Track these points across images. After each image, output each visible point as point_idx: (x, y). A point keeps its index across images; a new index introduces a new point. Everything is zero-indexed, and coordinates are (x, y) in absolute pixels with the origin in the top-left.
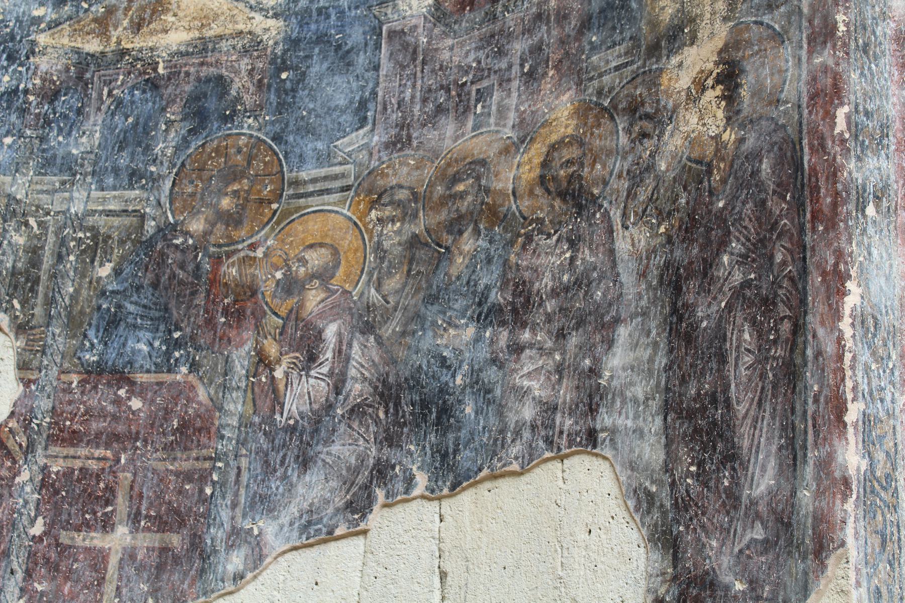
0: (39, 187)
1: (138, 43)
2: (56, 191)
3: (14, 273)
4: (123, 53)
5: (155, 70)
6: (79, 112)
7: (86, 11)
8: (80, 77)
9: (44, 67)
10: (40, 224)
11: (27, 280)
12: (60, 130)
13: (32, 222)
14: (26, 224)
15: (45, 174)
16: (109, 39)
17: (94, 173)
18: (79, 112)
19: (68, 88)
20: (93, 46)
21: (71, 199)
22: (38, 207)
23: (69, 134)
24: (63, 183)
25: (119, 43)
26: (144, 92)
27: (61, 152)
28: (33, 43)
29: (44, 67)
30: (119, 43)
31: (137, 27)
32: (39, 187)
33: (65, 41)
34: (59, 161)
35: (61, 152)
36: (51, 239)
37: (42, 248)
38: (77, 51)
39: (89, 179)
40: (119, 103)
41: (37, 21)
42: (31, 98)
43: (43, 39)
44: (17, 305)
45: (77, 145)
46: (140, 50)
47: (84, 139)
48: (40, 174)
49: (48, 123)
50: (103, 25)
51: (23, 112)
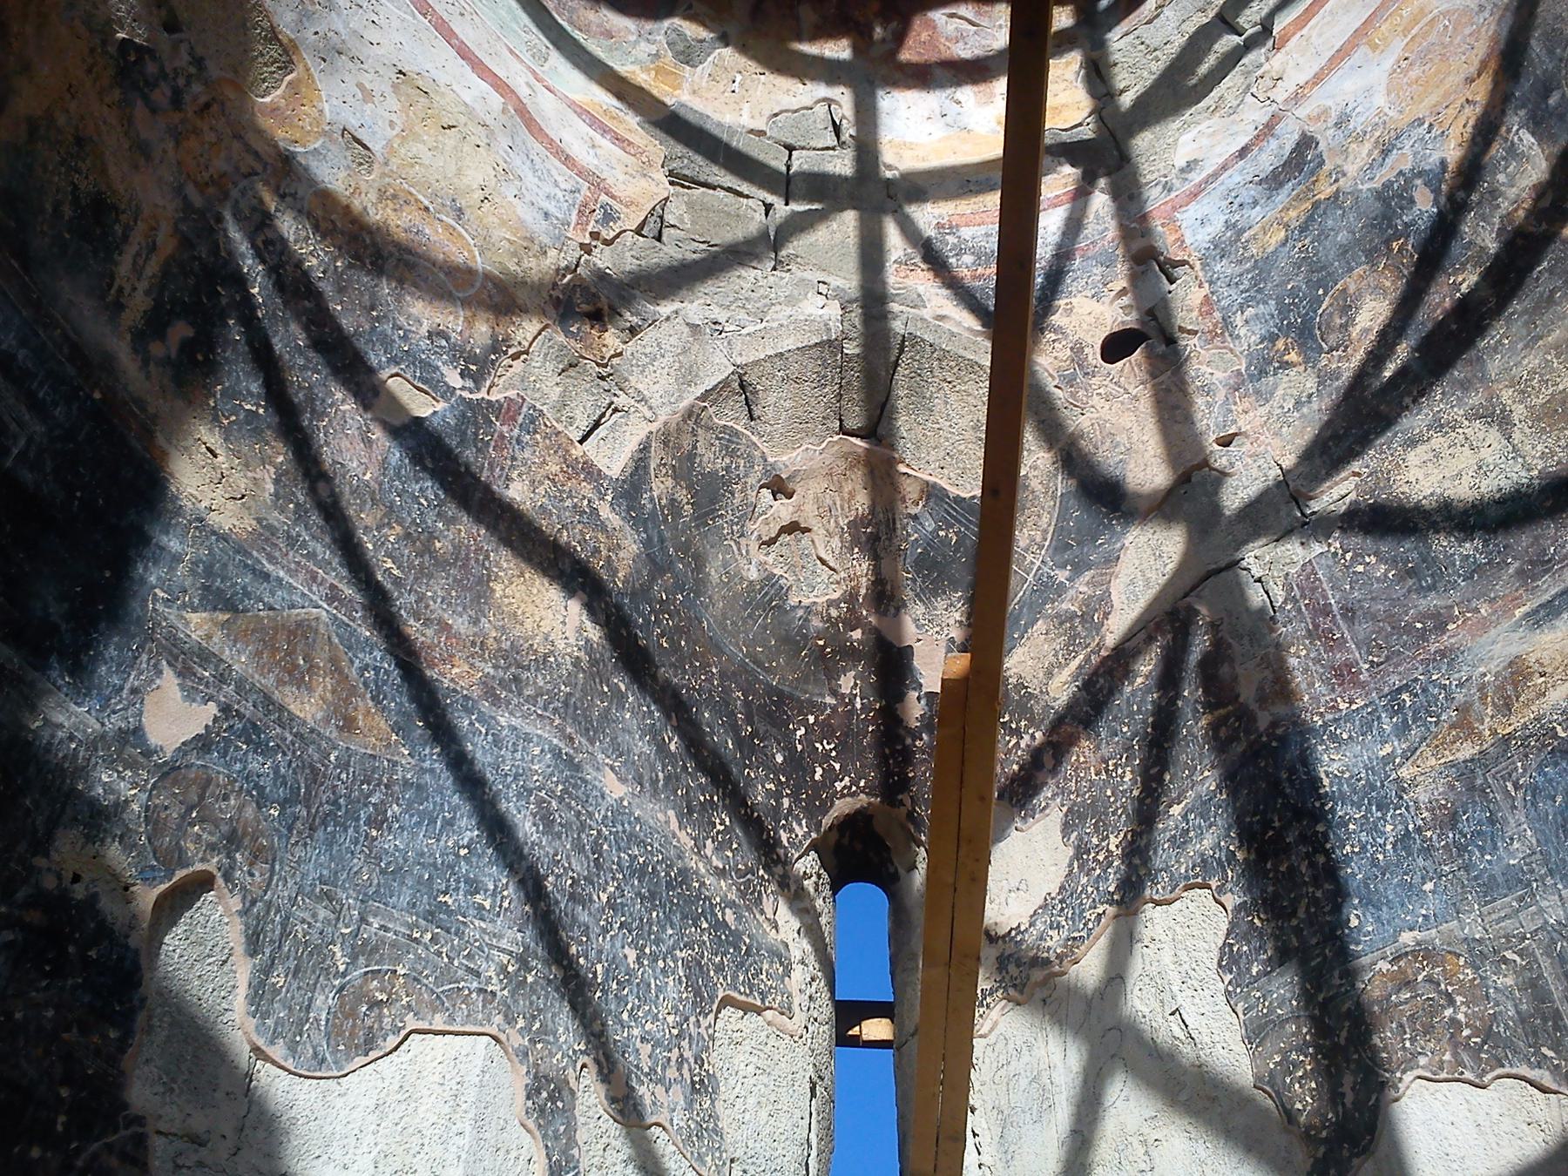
0: (1494, 916)
1: (1516, 722)
2: (1518, 911)
3: (1522, 1019)
4: (1506, 740)
5: (1555, 736)
6: (1492, 821)
7: (1437, 723)
8: (1471, 788)
9: (1423, 798)
10: (1520, 954)
11: (1545, 1020)
12: (1482, 850)
13: (1509, 955)
14: (1505, 960)
15: (1494, 900)
16: (1480, 735)
17: (1551, 872)
18: (1492, 821)
19: (1464, 805)
20: (1467, 751)
21: (1541, 911)
22: (1507, 937)
23: (1495, 848)
24: (1521, 899)
25: (1494, 733)
26: (1556, 764)
27: (1497, 871)
28: (1398, 780)
29: (1423, 798)
30: (1494, 733)
31: (1506, 707)
32: (1494, 916)
33: (1433, 761)
34: (1500, 880)
35: (1497, 871)
36: (1545, 963)
37: (1541, 976)
38: (1452, 764)
39: (1549, 881)
40: (1535, 790)
41: (1390, 757)
42: (1429, 834)
43: (1405, 772)
44: (1550, 1054)
45: (1512, 855)
46: (1525, 727)
47: (1516, 845)
48: (1487, 903)
49: (1462, 849)
50: (1465, 725)
51: (1427, 851)
